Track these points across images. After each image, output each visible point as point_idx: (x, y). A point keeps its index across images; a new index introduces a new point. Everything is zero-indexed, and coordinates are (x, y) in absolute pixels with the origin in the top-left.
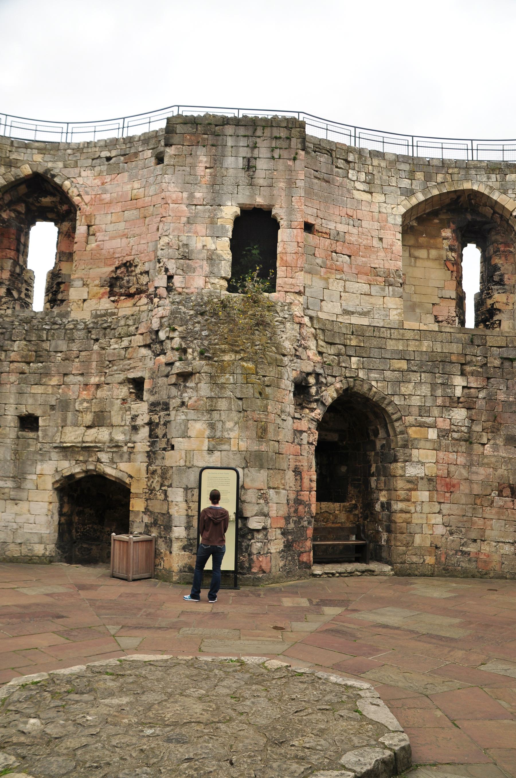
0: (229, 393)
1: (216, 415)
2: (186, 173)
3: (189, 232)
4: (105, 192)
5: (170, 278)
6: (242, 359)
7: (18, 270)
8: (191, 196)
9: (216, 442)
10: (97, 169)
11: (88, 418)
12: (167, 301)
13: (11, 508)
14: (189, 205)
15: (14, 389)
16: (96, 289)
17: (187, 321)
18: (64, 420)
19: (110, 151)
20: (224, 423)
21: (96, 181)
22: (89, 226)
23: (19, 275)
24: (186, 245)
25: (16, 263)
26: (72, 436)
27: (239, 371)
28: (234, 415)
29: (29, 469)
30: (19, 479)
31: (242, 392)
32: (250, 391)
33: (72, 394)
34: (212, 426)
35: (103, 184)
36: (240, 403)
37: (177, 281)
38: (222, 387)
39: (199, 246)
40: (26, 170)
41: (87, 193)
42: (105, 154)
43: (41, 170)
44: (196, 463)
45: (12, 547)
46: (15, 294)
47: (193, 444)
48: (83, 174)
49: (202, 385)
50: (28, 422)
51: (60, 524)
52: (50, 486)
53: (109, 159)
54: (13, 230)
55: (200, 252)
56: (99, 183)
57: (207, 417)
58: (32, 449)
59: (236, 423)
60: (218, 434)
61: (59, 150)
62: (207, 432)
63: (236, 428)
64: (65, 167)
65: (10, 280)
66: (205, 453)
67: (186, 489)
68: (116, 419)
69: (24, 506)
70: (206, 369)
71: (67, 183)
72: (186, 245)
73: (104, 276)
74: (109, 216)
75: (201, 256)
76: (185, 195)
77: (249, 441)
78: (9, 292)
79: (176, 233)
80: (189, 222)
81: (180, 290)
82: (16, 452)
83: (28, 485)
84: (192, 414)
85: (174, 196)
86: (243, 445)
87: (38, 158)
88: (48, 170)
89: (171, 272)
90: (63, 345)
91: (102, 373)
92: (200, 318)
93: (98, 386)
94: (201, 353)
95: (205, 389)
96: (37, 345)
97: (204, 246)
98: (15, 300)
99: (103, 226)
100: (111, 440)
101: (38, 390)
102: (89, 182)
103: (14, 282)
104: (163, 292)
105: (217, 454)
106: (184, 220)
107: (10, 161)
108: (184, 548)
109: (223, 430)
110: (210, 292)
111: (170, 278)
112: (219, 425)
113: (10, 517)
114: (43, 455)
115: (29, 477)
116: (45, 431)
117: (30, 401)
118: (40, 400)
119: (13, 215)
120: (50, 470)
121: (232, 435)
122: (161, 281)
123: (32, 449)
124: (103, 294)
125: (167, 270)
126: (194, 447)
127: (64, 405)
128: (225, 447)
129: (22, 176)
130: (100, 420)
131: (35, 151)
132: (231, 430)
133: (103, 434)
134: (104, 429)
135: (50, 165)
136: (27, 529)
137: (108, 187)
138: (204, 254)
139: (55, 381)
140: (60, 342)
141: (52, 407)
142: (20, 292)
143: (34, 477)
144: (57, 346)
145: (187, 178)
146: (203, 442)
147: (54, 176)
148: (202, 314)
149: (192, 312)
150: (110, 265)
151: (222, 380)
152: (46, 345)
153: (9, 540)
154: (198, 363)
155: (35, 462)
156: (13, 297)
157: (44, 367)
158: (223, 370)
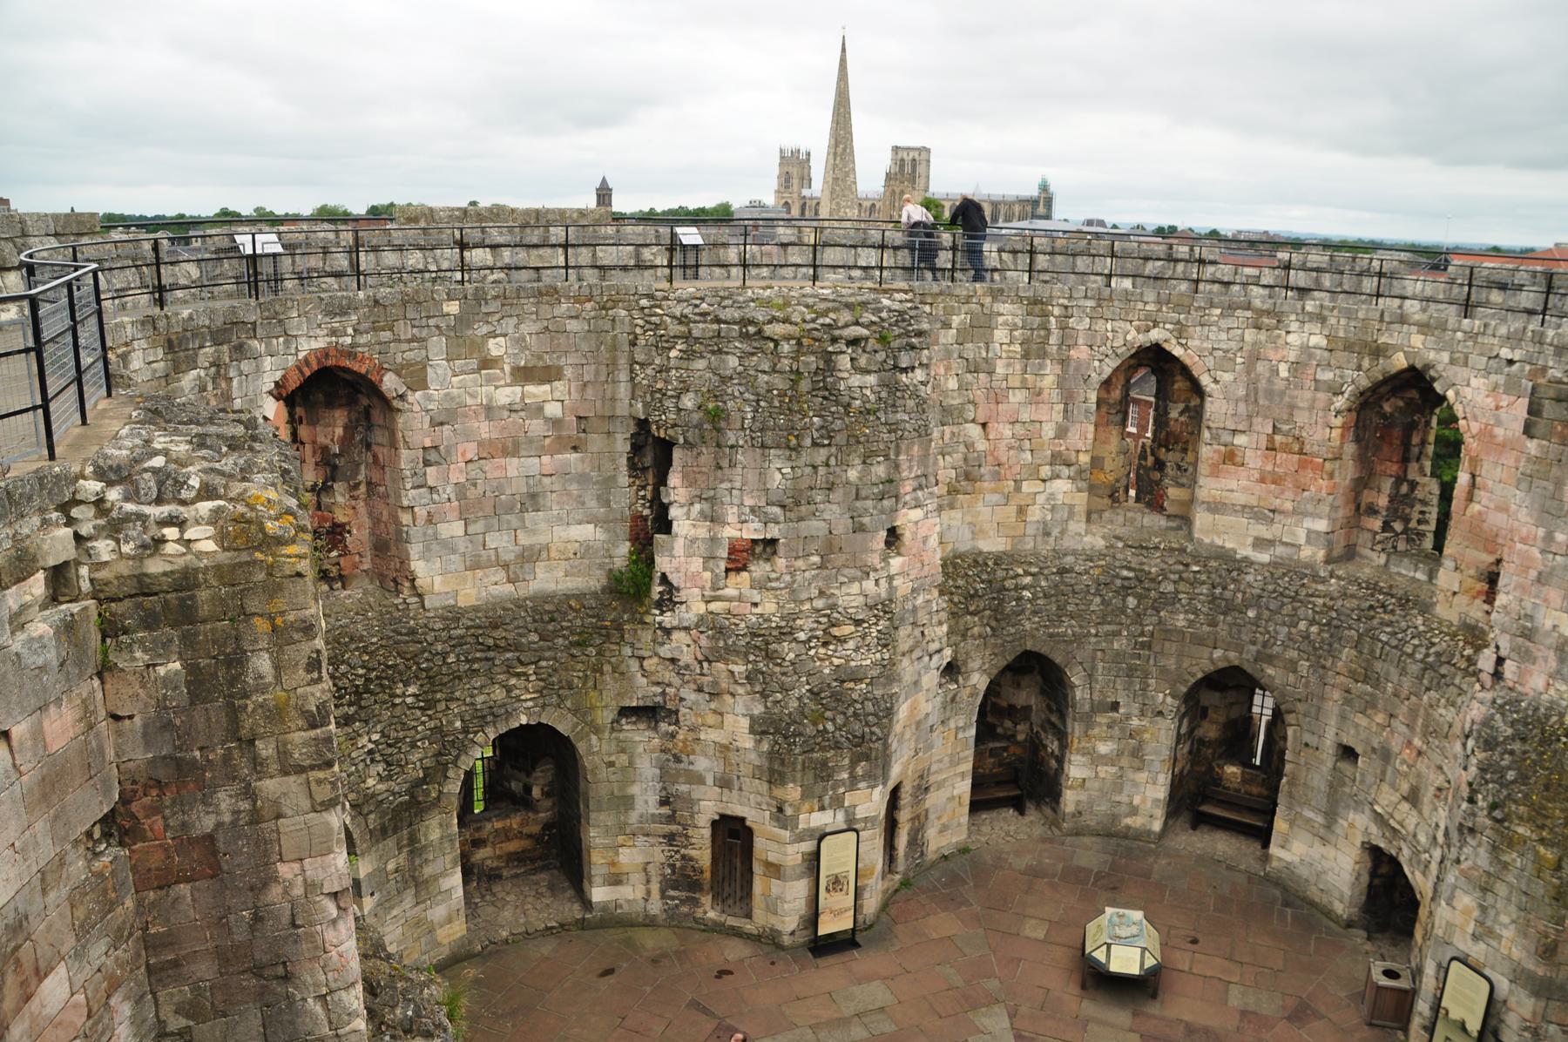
0: (1511, 879)
1: (1490, 898)
2: (1548, 494)
3: (1536, 597)
4: (1499, 423)
5: (1500, 661)
6: (1542, 841)
7: (1404, 489)
8: (1549, 537)
9: (1483, 933)
10: (1493, 377)
11: (1405, 787)
12: (1489, 696)
13: (1318, 850)
14: (1543, 552)
15: (1336, 710)
16: (1470, 582)
17: (1497, 744)
18: (1384, 773)
19: (1512, 349)
20: (1497, 913)
21: (1489, 400)
22: (1473, 476)
23: (1406, 495)
24: (1530, 617)
25: (1400, 480)
26: (1387, 799)
27: (1530, 856)
28: (1512, 908)
29: (1341, 811)
30: (1331, 816)
31: (1528, 885)
32: (1539, 889)
33: (1396, 744)
34: (1483, 909)
35: (1497, 408)
36: (1524, 899)
37: (1509, 668)
38: (1505, 866)
39: (1548, 624)
40: (1400, 362)
41: (1475, 418)
42: (1506, 353)
43: (1419, 366)
44: (1455, 941)
45: (1313, 889)
46: (1398, 526)
47: (1458, 919)
48: (1474, 382)
49: (1482, 850)
50: (1348, 753)
51: (1370, 886)
52: (1358, 844)
53: (1511, 362)
54: (1397, 432)
55: (1547, 634)
56: (1493, 405)
57: (1478, 894)
58: (1347, 790)
59: (1513, 922)
60: (1489, 923)
61: (1445, 330)
62: (1476, 913)
63: (1512, 927)
64: (1452, 362)
65: (1388, 509)
66: (1468, 937)
67: (1439, 966)
68: (1426, 809)
69: (1330, 851)
70: (1488, 832)
71: (1450, 394)
72: (1530, 617)
73: (1482, 567)
74: (1499, 469)
75: (1548, 641)
76: (1541, 532)
77: (1524, 954)
78: (1386, 526)
79: (1517, 594)
80: (1541, 580)
81: (1511, 684)
82: (1331, 786)
83: (1339, 830)
84: (1462, 882)
85: (1524, 530)
86: (1516, 953)
87: (1417, 340)
88: (1428, 366)
89: (1503, 653)
90: (1394, 673)
91: (1425, 735)
92: (1517, 746)
93: (1420, 753)
94: (1493, 806)
95: (1483, 859)
96: (1368, 661)
97: (1555, 627)
98: (1397, 534)
99: (1490, 483)
100: (1415, 836)
101: (1362, 720)
102: (1479, 399)
103: (1396, 510)
104: (1486, 679)
105: (1482, 946)
106: (1533, 574)
107: (1378, 347)
108: (1425, 1028)
109: (1495, 921)
110: (1552, 702)
111: (1500, 661)
112: (1492, 913)
113: (1317, 857)
114: (1358, 805)
115: (1341, 821)
116: (1362, 775)
117: (1352, 731)
118: (1363, 736)
119: (1401, 404)
120: (1358, 825)
121: (1505, 933)
122: (1486, 661)
123: (1347, 790)
124: (1479, 593)
125: (1497, 647)
126: (1458, 922)
127: (1386, 755)
128: (1494, 943)
129: (1394, 371)
130: (1413, 798)
131: (1414, 329)
132: (1506, 926)
133: (1412, 821)
134: (1414, 813)
135: (1432, 355)
136: (1331, 877)
137: (1502, 413)
138: (1552, 640)
139: (1380, 718)
140: (1392, 670)
141: (1374, 749)
142: (1406, 520)
143: (1345, 824)
144: (1387, 673)
145: (1548, 503)
146: (1468, 922)
147: (1433, 379)
148: (1524, 740)
149: (1510, 731)
150: (1491, 553)
151: (1506, 858)
152: (1378, 666)
153: (1313, 880)
154: (1483, 820)
155: (1348, 807)
156: (1393, 530)
157: (1371, 695)
158: (1511, 845)
